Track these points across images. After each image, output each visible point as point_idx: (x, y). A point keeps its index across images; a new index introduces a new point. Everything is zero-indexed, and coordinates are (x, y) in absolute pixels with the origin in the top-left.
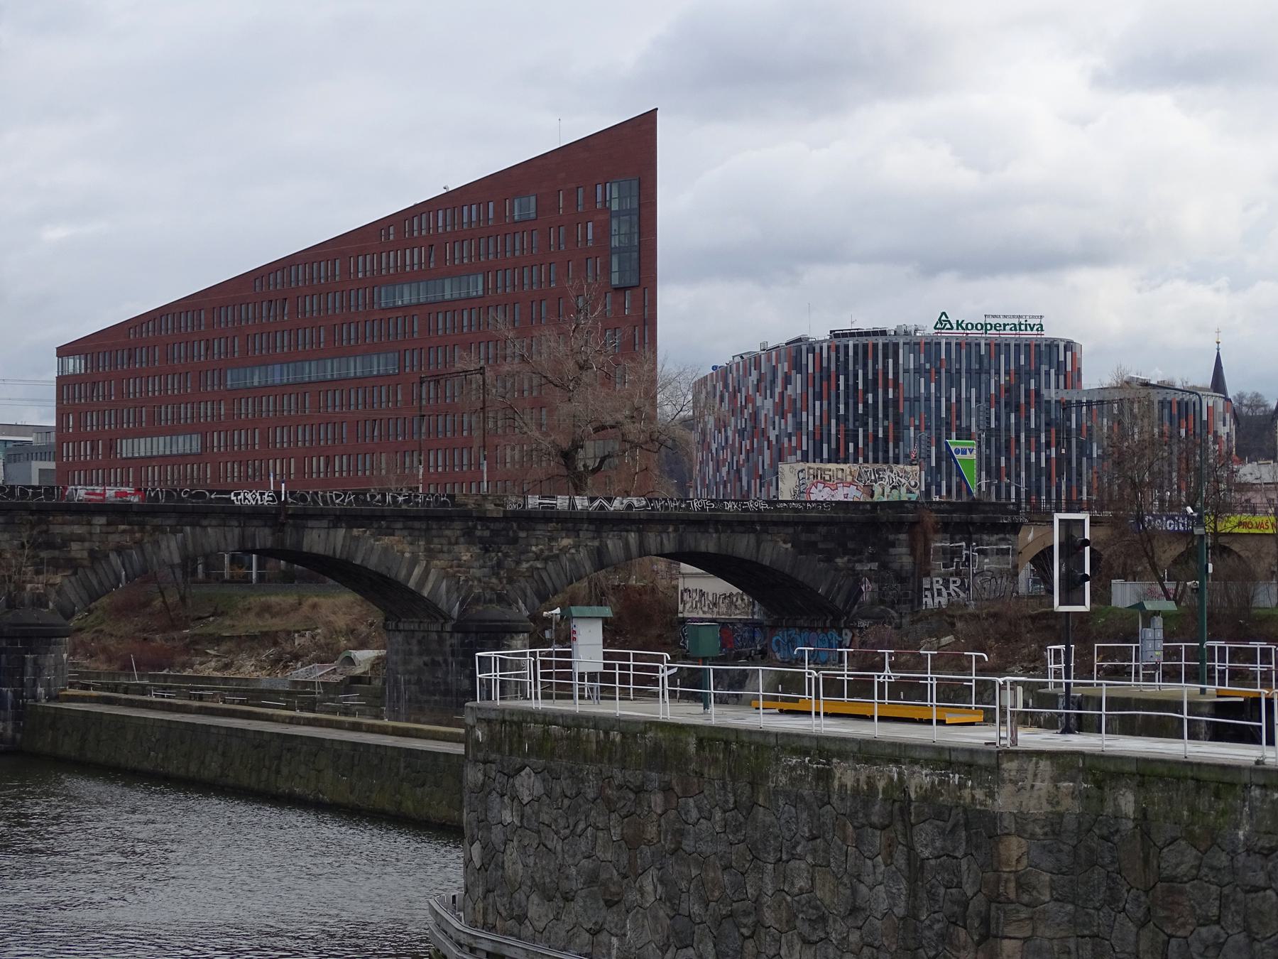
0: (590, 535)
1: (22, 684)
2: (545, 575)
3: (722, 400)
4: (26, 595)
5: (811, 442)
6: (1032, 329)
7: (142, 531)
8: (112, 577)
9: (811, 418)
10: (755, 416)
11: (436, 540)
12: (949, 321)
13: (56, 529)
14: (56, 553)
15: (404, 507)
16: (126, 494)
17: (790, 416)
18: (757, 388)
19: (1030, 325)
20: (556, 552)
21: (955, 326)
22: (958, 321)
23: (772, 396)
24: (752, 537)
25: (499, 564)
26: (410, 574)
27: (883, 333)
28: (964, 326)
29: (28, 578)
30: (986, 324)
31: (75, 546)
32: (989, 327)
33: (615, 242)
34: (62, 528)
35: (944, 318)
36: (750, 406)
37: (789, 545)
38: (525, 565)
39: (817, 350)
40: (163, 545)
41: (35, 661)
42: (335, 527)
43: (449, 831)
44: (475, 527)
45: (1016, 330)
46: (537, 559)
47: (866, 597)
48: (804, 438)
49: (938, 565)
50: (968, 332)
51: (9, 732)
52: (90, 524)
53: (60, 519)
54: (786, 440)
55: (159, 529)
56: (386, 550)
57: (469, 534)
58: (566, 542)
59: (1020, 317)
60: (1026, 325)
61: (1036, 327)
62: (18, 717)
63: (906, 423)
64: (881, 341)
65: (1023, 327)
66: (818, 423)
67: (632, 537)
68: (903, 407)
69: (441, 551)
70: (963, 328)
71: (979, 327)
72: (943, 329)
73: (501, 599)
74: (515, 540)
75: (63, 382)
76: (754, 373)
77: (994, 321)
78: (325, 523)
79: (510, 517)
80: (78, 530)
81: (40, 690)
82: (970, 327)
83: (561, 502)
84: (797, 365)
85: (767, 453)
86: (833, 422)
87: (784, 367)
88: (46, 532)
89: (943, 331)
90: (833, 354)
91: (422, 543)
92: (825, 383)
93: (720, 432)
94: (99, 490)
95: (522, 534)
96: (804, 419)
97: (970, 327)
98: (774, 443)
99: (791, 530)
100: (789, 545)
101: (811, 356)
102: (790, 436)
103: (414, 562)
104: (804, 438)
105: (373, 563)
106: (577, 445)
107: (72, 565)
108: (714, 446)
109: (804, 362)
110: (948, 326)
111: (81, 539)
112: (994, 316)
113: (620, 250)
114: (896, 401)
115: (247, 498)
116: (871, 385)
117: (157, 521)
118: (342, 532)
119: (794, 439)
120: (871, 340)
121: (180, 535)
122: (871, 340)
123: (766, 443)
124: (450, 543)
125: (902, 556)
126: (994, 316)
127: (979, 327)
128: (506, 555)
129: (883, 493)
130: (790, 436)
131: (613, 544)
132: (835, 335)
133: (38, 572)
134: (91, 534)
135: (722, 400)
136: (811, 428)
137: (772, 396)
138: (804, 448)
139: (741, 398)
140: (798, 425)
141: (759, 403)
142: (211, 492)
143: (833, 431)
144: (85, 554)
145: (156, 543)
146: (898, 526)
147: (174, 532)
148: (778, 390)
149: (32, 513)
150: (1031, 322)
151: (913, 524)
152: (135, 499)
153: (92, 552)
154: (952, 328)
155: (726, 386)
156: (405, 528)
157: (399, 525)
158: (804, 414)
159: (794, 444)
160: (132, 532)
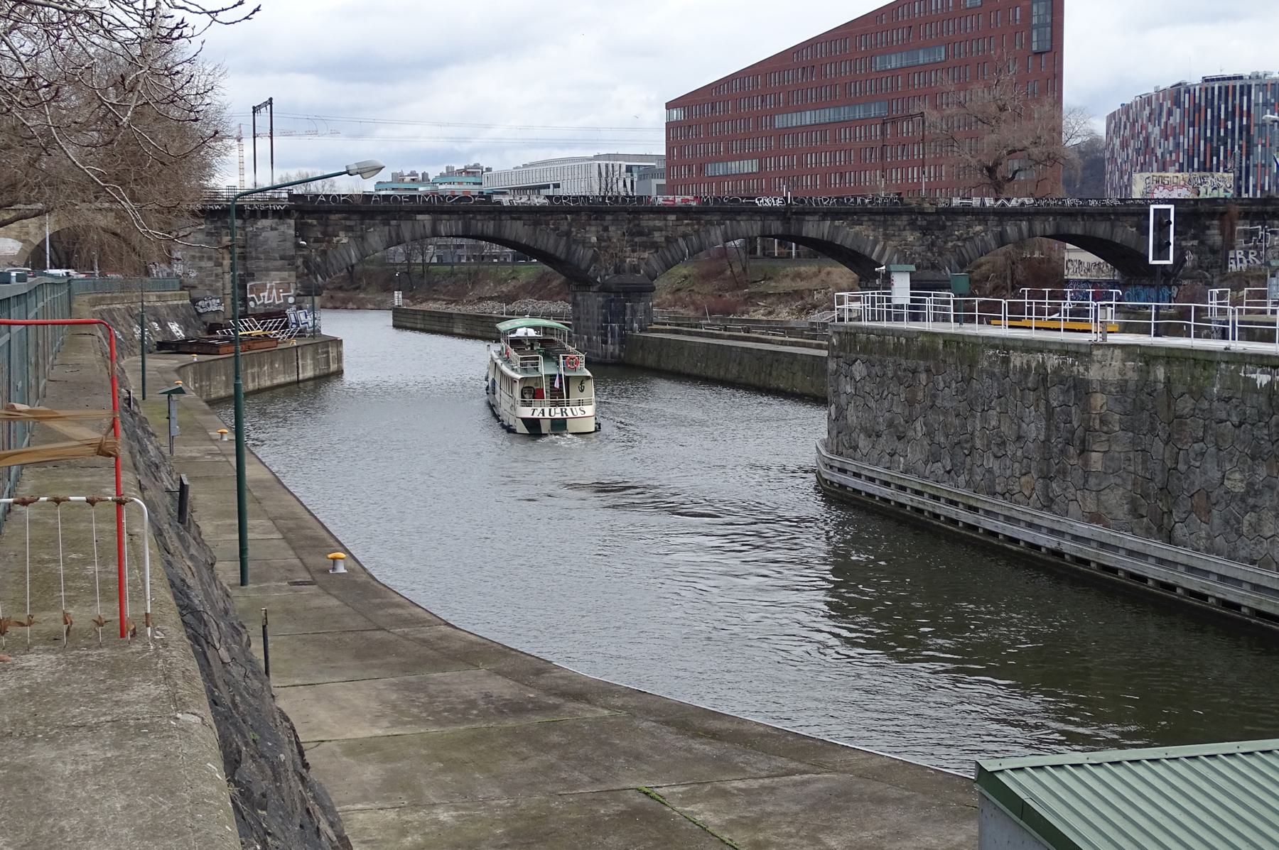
0: (995, 223)
1: (624, 322)
2: (964, 251)
3: (1125, 128)
4: (626, 266)
7: (699, 224)
8: (680, 253)
9: (1186, 140)
10: (1147, 139)
11: (890, 228)
13: (644, 223)
14: (644, 239)
15: (869, 206)
16: (688, 200)
17: (1171, 139)
18: (1149, 120)
20: (971, 235)
24: (1108, 224)
25: (933, 244)
26: (873, 251)
27: (1241, 78)
29: (628, 254)
31: (656, 234)
33: (1035, 21)
34: (647, 222)
37: (1134, 229)
38: (950, 244)
39: (1192, 91)
40: (712, 233)
41: (632, 306)
42: (824, 220)
43: (819, 400)
44: (917, 219)
46: (959, 240)
47: (1188, 264)
48: (1181, 154)
49: (1240, 242)
51: (617, 351)
52: (665, 219)
53: (646, 217)
55: (710, 223)
56: (856, 234)
57: (913, 225)
58: (978, 228)
62: (622, 343)
63: (1255, 142)
64: (1238, 83)
66: (1191, 143)
67: (1024, 224)
68: (1254, 131)
69: (894, 235)
73: (934, 267)
74: (943, 228)
75: (670, 126)
76: (1147, 108)
78: (817, 218)
79: (939, 212)
80: (658, 223)
81: (636, 325)
83: (976, 202)
84: (1177, 102)
87: (1167, 104)
88: (638, 225)
90: (1203, 94)
91: (881, 230)
92: (1197, 115)
94: (671, 198)
95: (949, 224)
96: (1181, 141)
99: (1136, 219)
100: (1134, 229)
101: (1187, 95)
102: (1171, 153)
103: (876, 242)
104: (1181, 154)
105: (848, 243)
106: (997, 164)
107: (655, 246)
108: (1119, 161)
109: (1182, 100)
111: (660, 229)
113: (1038, 26)
114: (1248, 126)
115: (765, 202)
116: (1231, 115)
117: (708, 217)
118: (828, 223)
119: (1174, 155)
120: (1231, 83)
121: (723, 227)
122: (1231, 83)
124: (900, 230)
125: (1215, 236)
128: (938, 237)
129: (1206, 192)
130: (1171, 153)
131: (1011, 229)
132: (1206, 80)
133: (634, 251)
134: (666, 226)
135: (1125, 128)
136: (1186, 147)
138: (1181, 161)
139: (1138, 127)
141: (1150, 130)
142: (742, 198)
143: (1202, 149)
144: (663, 239)
145: (708, 232)
146: (1212, 215)
147: (719, 224)
148: (1163, 120)
149: (629, 214)
151: (1223, 214)
152: (694, 204)
153: (667, 238)
155: (1128, 118)
156: (870, 220)
157: (866, 218)
158: (1181, 137)
159: (1174, 158)
160: (692, 225)
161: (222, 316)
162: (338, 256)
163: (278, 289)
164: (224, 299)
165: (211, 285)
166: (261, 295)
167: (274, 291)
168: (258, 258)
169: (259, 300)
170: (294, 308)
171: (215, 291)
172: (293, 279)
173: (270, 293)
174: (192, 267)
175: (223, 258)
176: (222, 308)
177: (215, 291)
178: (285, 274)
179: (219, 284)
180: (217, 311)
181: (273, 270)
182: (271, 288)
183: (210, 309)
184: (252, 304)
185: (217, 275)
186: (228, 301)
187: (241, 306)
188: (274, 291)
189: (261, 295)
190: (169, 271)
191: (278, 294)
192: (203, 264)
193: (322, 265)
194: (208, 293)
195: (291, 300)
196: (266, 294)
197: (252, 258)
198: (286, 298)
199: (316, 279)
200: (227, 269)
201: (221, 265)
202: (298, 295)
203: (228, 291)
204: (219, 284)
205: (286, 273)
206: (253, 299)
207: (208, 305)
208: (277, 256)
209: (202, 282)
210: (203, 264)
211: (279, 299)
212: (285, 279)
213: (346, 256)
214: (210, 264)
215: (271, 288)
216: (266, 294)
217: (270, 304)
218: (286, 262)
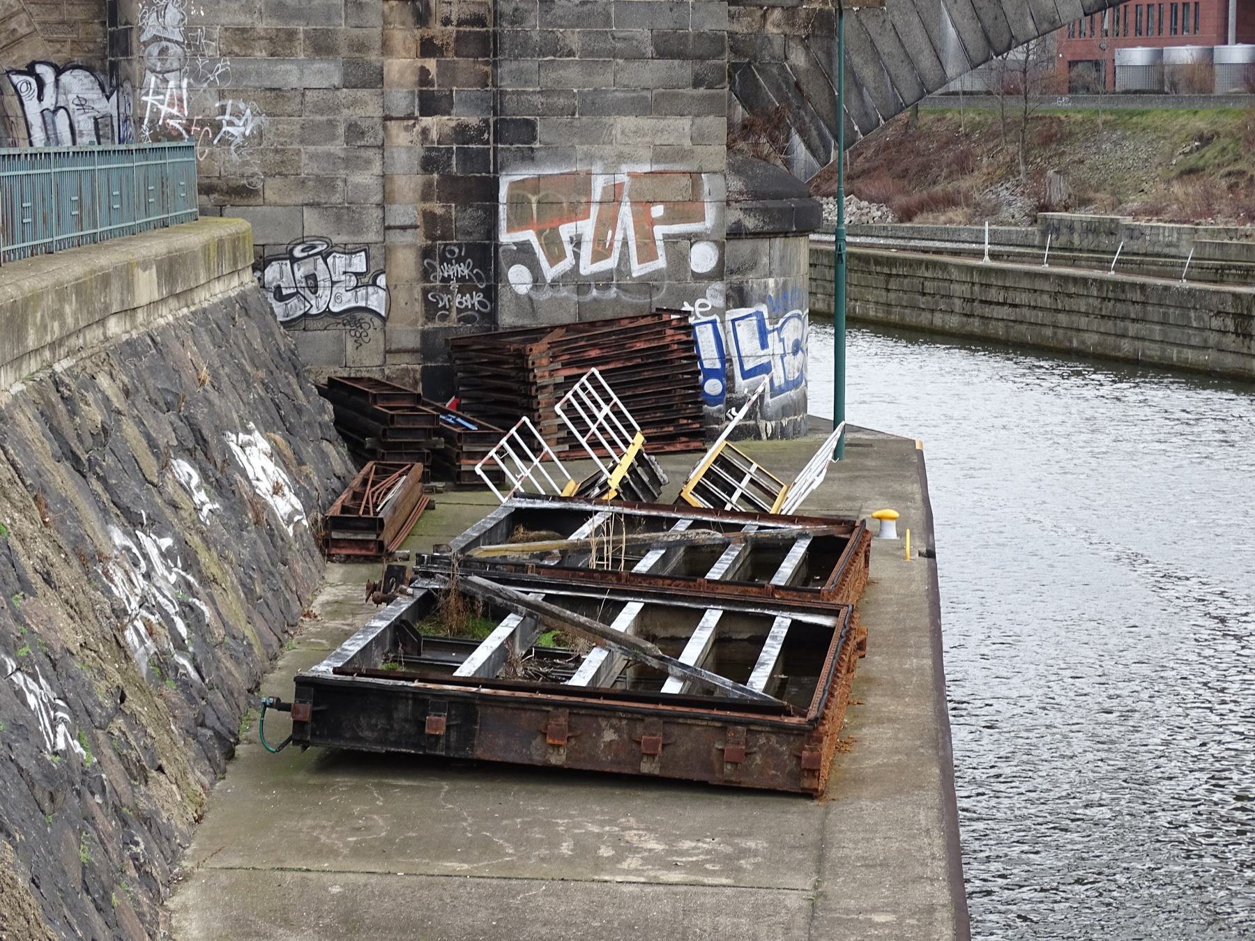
161: (374, 335)
162: (886, 45)
163: (642, 204)
164: (388, 251)
165: (326, 183)
166: (566, 231)
167: (626, 211)
168: (553, 48)
169: (555, 256)
170: (714, 296)
171: (346, 214)
172: (716, 154)
173: (608, 222)
174: (232, 88)
175: (386, 48)
176: (376, 300)
177: (346, 214)
178: (679, 128)
179: (366, 179)
180: (353, 316)
181: (620, 108)
182: (613, 198)
183: (317, 304)
184: (518, 277)
185: (355, 131)
186: (406, 262)
187: (466, 286)
188: (626, 211)
189: (566, 231)
190: (108, 107)
191: (644, 226)
192: (289, 74)
193: (813, 87)
194: (313, 223)
195: (703, 258)
196: (587, 228)
197: (525, 48)
198: (678, 246)
199: (785, 151)
200: (402, 99)
201: (376, 80)
202: (736, 233)
203: (407, 210)
204: (366, 179)
205: (685, 123)
206: (524, 253)
207: (312, 282)
208: (643, 34)
209: (281, 167)
210: (289, 74)
211: (647, 253)
212: (681, 154)
213: (917, 40)
214: (325, 74)
215: (613, 198)
216: (587, 228)
217: (604, 279)
218: (683, 70)
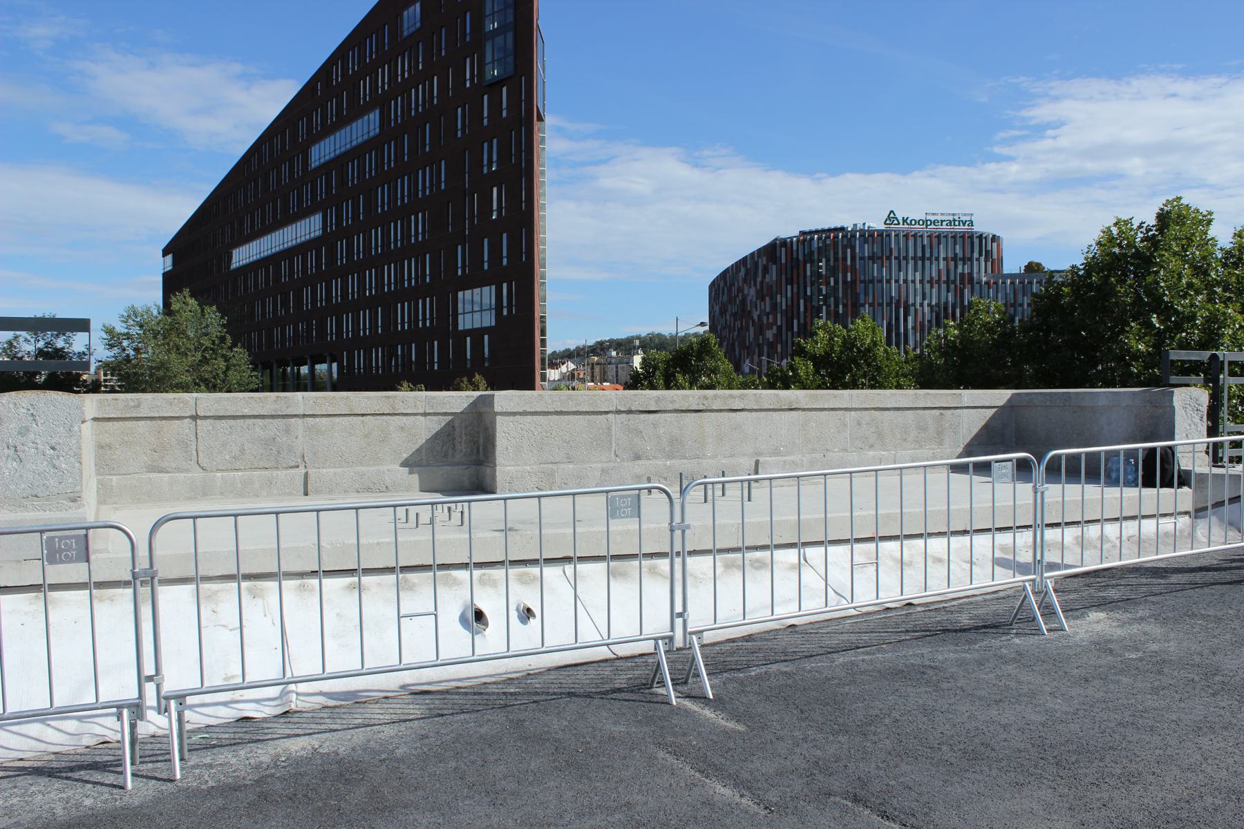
3: (723, 294)
5: (784, 319)
6: (964, 225)
9: (784, 300)
10: (743, 302)
12: (896, 218)
17: (767, 299)
18: (745, 280)
19: (962, 221)
21: (901, 223)
22: (903, 218)
23: (755, 285)
27: (842, 229)
28: (909, 222)
30: (927, 221)
32: (929, 223)
35: (892, 215)
36: (740, 294)
39: (789, 245)
45: (951, 225)
48: (779, 315)
50: (912, 227)
54: (765, 318)
59: (954, 215)
60: (959, 221)
61: (967, 223)
63: (862, 301)
65: (957, 223)
66: (789, 303)
68: (860, 288)
70: (908, 224)
71: (921, 223)
72: (891, 224)
76: (743, 269)
77: (933, 218)
82: (913, 222)
85: (752, 329)
86: (802, 302)
89: (891, 226)
90: (801, 247)
92: (795, 271)
93: (722, 317)
96: (779, 300)
97: (913, 222)
98: (756, 321)
101: (783, 249)
104: (779, 315)
108: (719, 327)
109: (778, 255)
110: (896, 222)
112: (934, 214)
114: (854, 282)
119: (771, 317)
123: (751, 321)
126: (934, 214)
127: (921, 223)
130: (768, 315)
132: (803, 233)
135: (723, 294)
136: (784, 307)
137: (755, 285)
138: (779, 324)
139: (734, 289)
140: (774, 306)
141: (746, 292)
143: (802, 309)
148: (759, 279)
150: (963, 218)
154: (899, 224)
155: (725, 283)
158: (779, 296)
159: (771, 320)
